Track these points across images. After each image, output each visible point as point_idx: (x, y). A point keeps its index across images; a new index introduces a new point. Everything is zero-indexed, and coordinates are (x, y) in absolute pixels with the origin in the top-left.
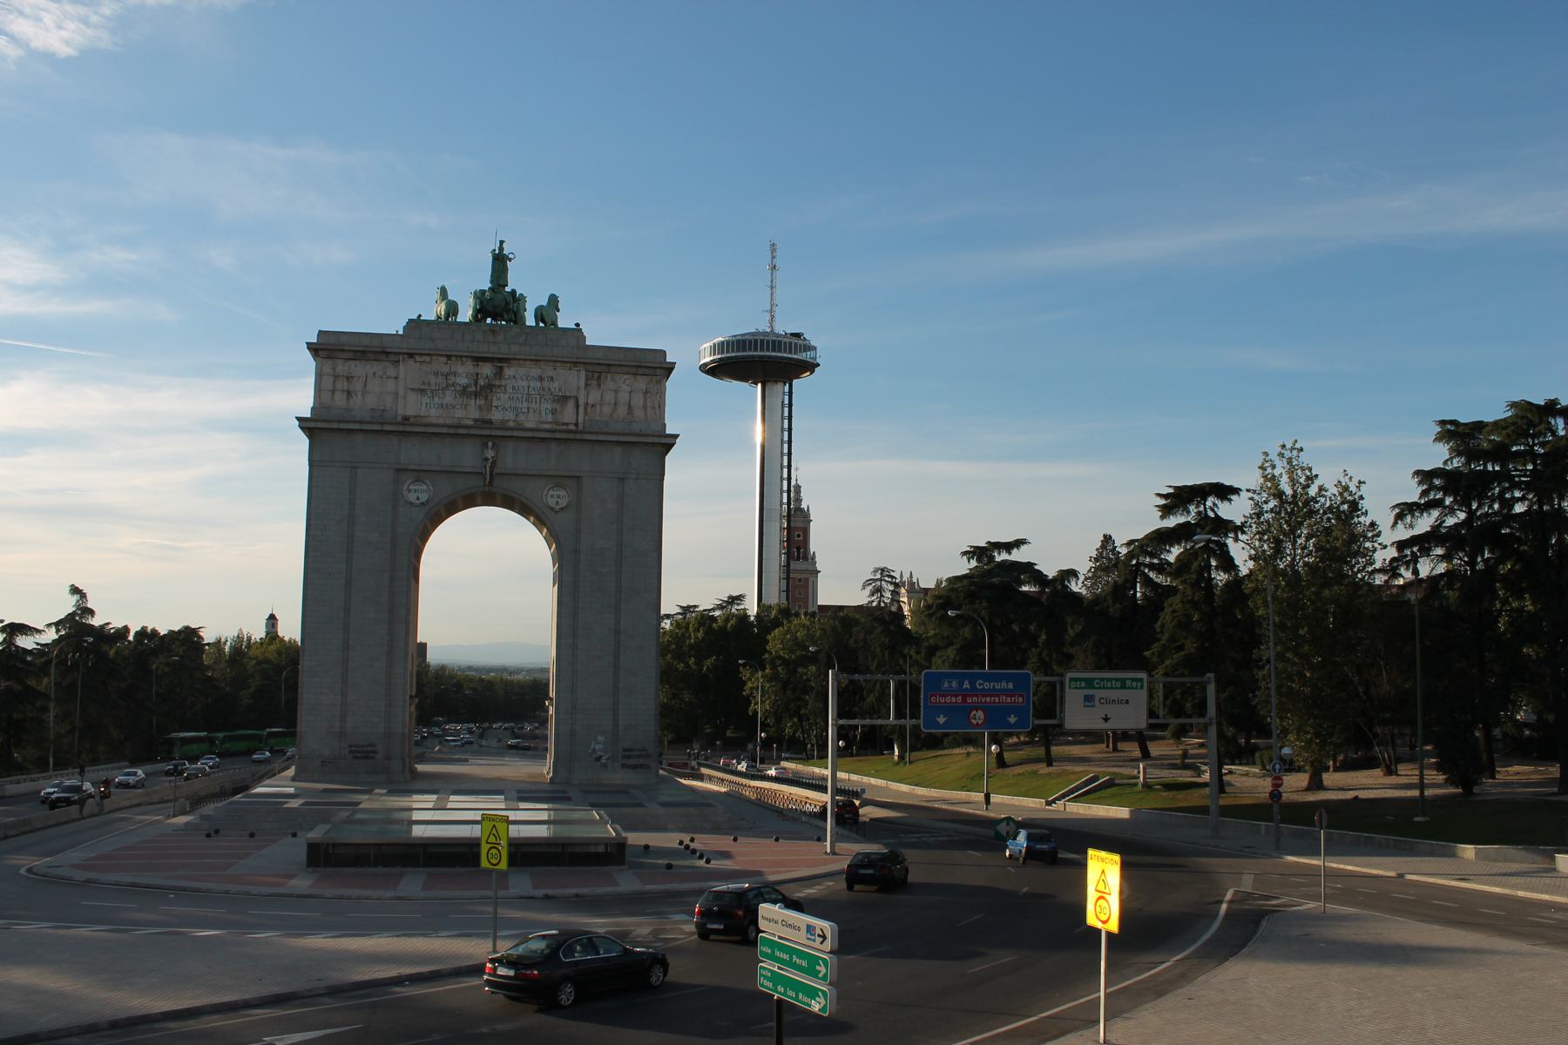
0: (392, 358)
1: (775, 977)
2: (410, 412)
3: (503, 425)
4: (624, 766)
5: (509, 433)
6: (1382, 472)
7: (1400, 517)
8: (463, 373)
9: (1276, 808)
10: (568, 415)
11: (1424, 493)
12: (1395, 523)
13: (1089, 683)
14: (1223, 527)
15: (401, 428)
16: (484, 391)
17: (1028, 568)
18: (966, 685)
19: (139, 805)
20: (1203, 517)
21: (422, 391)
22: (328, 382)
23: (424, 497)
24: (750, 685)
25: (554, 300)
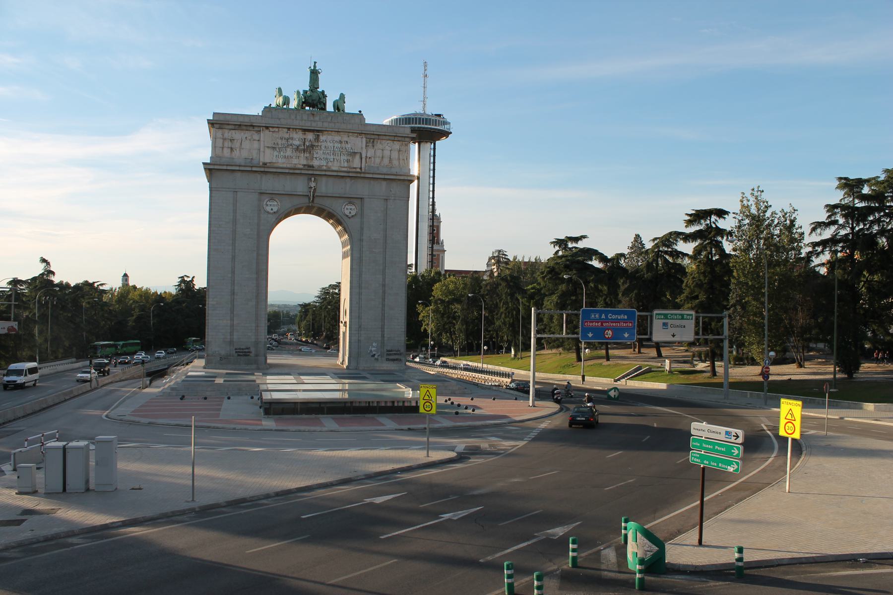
0: (256, 129)
1: (702, 457)
2: (267, 160)
3: (320, 168)
4: (388, 360)
5: (323, 173)
6: (807, 204)
7: (814, 229)
8: (297, 138)
9: (765, 384)
10: (356, 163)
11: (829, 217)
12: (811, 232)
13: (666, 316)
14: (721, 232)
15: (262, 169)
16: (309, 149)
17: (590, 253)
18: (603, 316)
19: (111, 383)
20: (709, 227)
21: (274, 148)
22: (220, 143)
23: (275, 209)
24: (422, 314)
25: (342, 97)
